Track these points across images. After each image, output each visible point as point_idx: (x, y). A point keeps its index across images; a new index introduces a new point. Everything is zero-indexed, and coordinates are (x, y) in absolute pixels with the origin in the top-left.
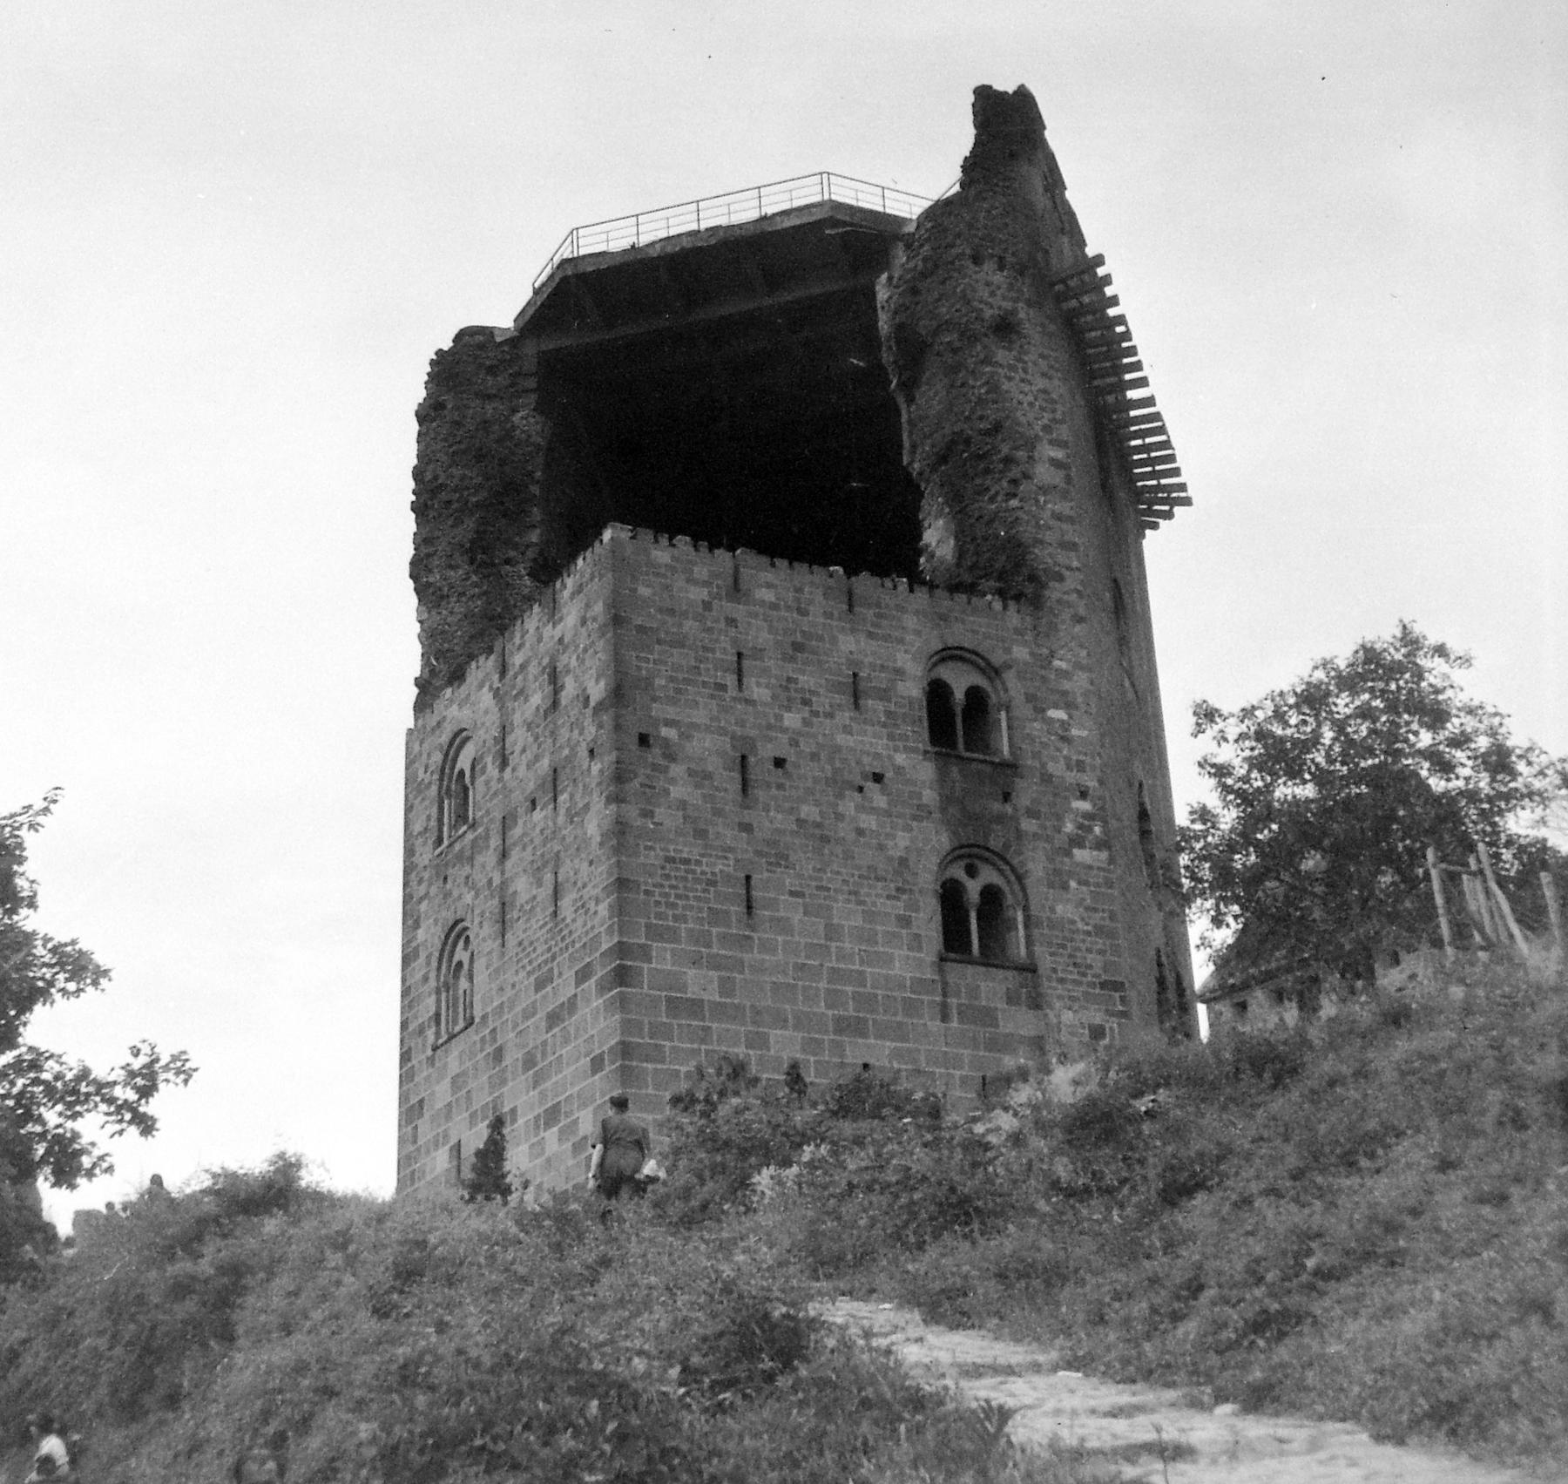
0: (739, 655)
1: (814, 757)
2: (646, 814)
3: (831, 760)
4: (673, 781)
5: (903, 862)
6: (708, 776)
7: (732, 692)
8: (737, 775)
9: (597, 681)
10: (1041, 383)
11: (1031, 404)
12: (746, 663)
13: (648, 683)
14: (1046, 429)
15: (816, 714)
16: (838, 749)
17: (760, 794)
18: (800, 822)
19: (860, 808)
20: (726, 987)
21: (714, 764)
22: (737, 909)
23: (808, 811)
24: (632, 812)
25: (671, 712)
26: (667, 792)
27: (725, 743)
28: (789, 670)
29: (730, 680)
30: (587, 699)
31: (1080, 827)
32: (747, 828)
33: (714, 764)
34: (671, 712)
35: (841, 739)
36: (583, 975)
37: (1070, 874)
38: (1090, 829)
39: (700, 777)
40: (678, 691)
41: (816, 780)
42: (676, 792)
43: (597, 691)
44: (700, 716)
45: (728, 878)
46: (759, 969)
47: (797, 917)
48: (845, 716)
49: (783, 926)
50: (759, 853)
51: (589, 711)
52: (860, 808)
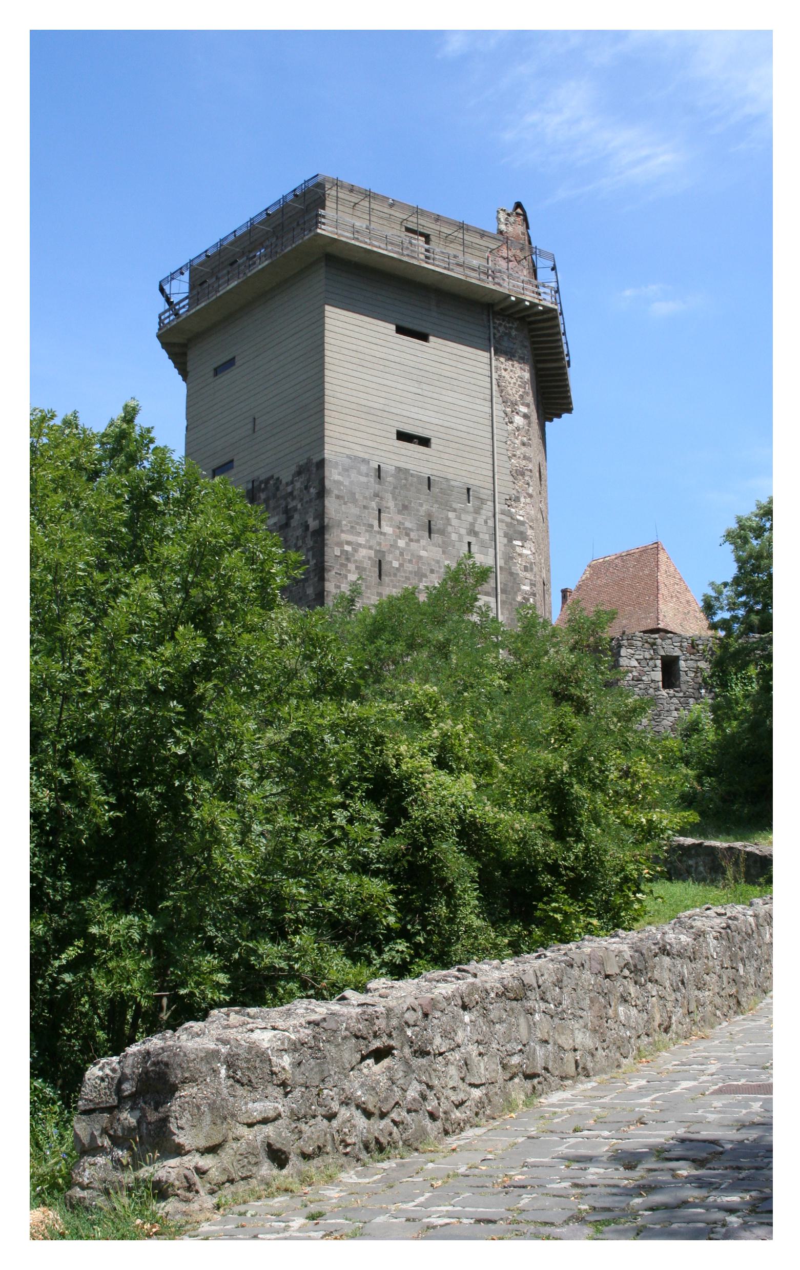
0: (380, 511)
1: (410, 561)
3: (417, 563)
4: (349, 571)
6: (364, 569)
7: (376, 528)
8: (377, 570)
9: (314, 519)
11: (515, 384)
12: (382, 514)
13: (339, 524)
15: (411, 540)
16: (420, 557)
17: (386, 579)
25: (350, 538)
26: (346, 577)
27: (372, 553)
28: (399, 518)
29: (376, 523)
30: (307, 527)
31: (524, 598)
33: (367, 564)
34: (350, 538)
35: (423, 553)
38: (528, 600)
40: (352, 527)
41: (411, 572)
44: (361, 540)
48: (423, 542)
51: (309, 534)
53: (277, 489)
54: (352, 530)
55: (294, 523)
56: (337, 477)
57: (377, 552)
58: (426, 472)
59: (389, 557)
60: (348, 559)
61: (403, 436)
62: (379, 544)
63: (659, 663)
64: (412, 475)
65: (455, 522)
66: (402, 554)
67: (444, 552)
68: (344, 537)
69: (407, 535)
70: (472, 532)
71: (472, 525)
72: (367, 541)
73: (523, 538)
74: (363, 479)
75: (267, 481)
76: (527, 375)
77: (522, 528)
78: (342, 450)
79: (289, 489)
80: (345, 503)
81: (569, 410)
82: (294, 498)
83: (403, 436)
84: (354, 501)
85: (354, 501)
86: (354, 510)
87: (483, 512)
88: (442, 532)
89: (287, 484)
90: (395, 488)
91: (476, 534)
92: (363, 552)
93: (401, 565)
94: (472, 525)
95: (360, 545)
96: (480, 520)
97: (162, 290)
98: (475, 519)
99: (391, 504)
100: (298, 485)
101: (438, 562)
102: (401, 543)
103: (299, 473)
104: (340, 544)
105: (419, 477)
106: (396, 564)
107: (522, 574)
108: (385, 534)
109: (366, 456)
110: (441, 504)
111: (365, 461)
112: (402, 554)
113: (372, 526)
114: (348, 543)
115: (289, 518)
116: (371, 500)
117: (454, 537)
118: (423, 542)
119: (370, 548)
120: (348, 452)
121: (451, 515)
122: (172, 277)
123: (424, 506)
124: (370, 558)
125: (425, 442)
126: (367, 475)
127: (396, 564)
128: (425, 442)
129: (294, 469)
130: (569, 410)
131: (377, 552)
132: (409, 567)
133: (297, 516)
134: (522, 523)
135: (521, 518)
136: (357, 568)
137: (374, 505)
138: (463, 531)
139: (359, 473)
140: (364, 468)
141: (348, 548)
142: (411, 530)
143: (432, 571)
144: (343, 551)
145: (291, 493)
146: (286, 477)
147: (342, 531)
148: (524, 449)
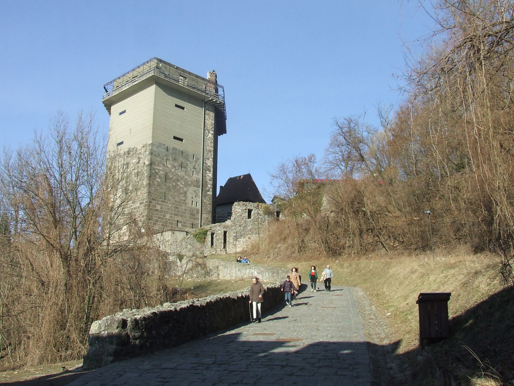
1: (175, 176)
2: (153, 182)
3: (177, 176)
4: (157, 178)
5: (185, 192)
7: (166, 165)
9: (147, 161)
10: (211, 121)
14: (211, 128)
15: (176, 169)
18: (173, 185)
19: (180, 184)
20: (161, 208)
21: (162, 176)
22: (164, 197)
23: (174, 184)
24: (151, 183)
28: (173, 162)
29: (165, 164)
30: (145, 163)
32: (166, 185)
33: (162, 176)
34: (158, 168)
35: (179, 174)
36: (141, 203)
37: (207, 196)
39: (160, 178)
41: (175, 179)
42: (157, 180)
43: (147, 163)
44: (161, 169)
45: (163, 193)
46: (165, 205)
47: (171, 199)
49: (169, 200)
50: (167, 189)
52: (180, 184)
53: (136, 151)
54: (158, 165)
55: (141, 162)
56: (155, 149)
57: (165, 172)
58: (182, 149)
59: (169, 174)
60: (157, 174)
61: (175, 138)
62: (166, 170)
63: (247, 211)
64: (177, 150)
65: (189, 165)
66: (173, 173)
67: (185, 174)
68: (156, 167)
69: (175, 168)
70: (194, 168)
71: (194, 166)
72: (163, 169)
73: (210, 171)
74: (162, 150)
75: (133, 149)
76: (213, 122)
77: (209, 168)
78: (157, 141)
79: (140, 151)
80: (157, 157)
81: (225, 133)
82: (141, 155)
83: (175, 138)
84: (159, 156)
85: (159, 156)
86: (159, 159)
87: (198, 162)
88: (185, 168)
89: (139, 150)
90: (172, 153)
91: (195, 169)
92: (161, 172)
93: (173, 177)
94: (194, 166)
95: (161, 170)
96: (197, 165)
97: (105, 88)
98: (195, 164)
99: (170, 158)
100: (143, 151)
101: (183, 176)
102: (173, 170)
103: (143, 147)
104: (154, 169)
105: (179, 150)
106: (171, 176)
107: (209, 181)
108: (168, 167)
109: (163, 143)
110: (185, 159)
111: (164, 145)
112: (173, 173)
113: (164, 164)
114: (157, 169)
115: (140, 160)
116: (165, 156)
117: (189, 169)
118: (179, 170)
119: (164, 171)
120: (159, 142)
121: (188, 162)
122: (108, 84)
123: (181, 159)
124: (163, 174)
125: (181, 140)
126: (164, 149)
127: (171, 176)
128: (181, 140)
129: (142, 146)
130: (225, 133)
131: (165, 172)
132: (175, 177)
133: (142, 160)
134: (210, 166)
135: (209, 165)
136: (159, 177)
137: (165, 158)
138: (192, 168)
139: (161, 148)
140: (163, 147)
141: (157, 171)
142: (176, 166)
143: (182, 179)
144: (155, 172)
145: (141, 153)
146: (139, 148)
147: (156, 166)
148: (211, 144)
